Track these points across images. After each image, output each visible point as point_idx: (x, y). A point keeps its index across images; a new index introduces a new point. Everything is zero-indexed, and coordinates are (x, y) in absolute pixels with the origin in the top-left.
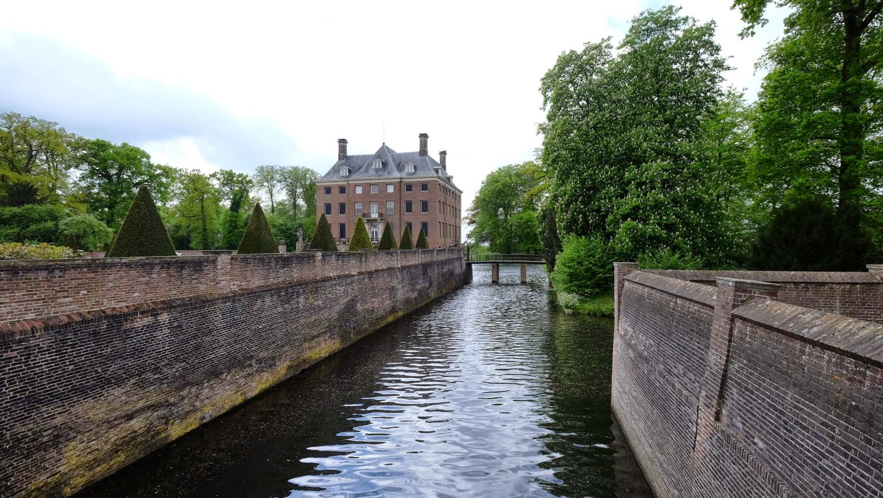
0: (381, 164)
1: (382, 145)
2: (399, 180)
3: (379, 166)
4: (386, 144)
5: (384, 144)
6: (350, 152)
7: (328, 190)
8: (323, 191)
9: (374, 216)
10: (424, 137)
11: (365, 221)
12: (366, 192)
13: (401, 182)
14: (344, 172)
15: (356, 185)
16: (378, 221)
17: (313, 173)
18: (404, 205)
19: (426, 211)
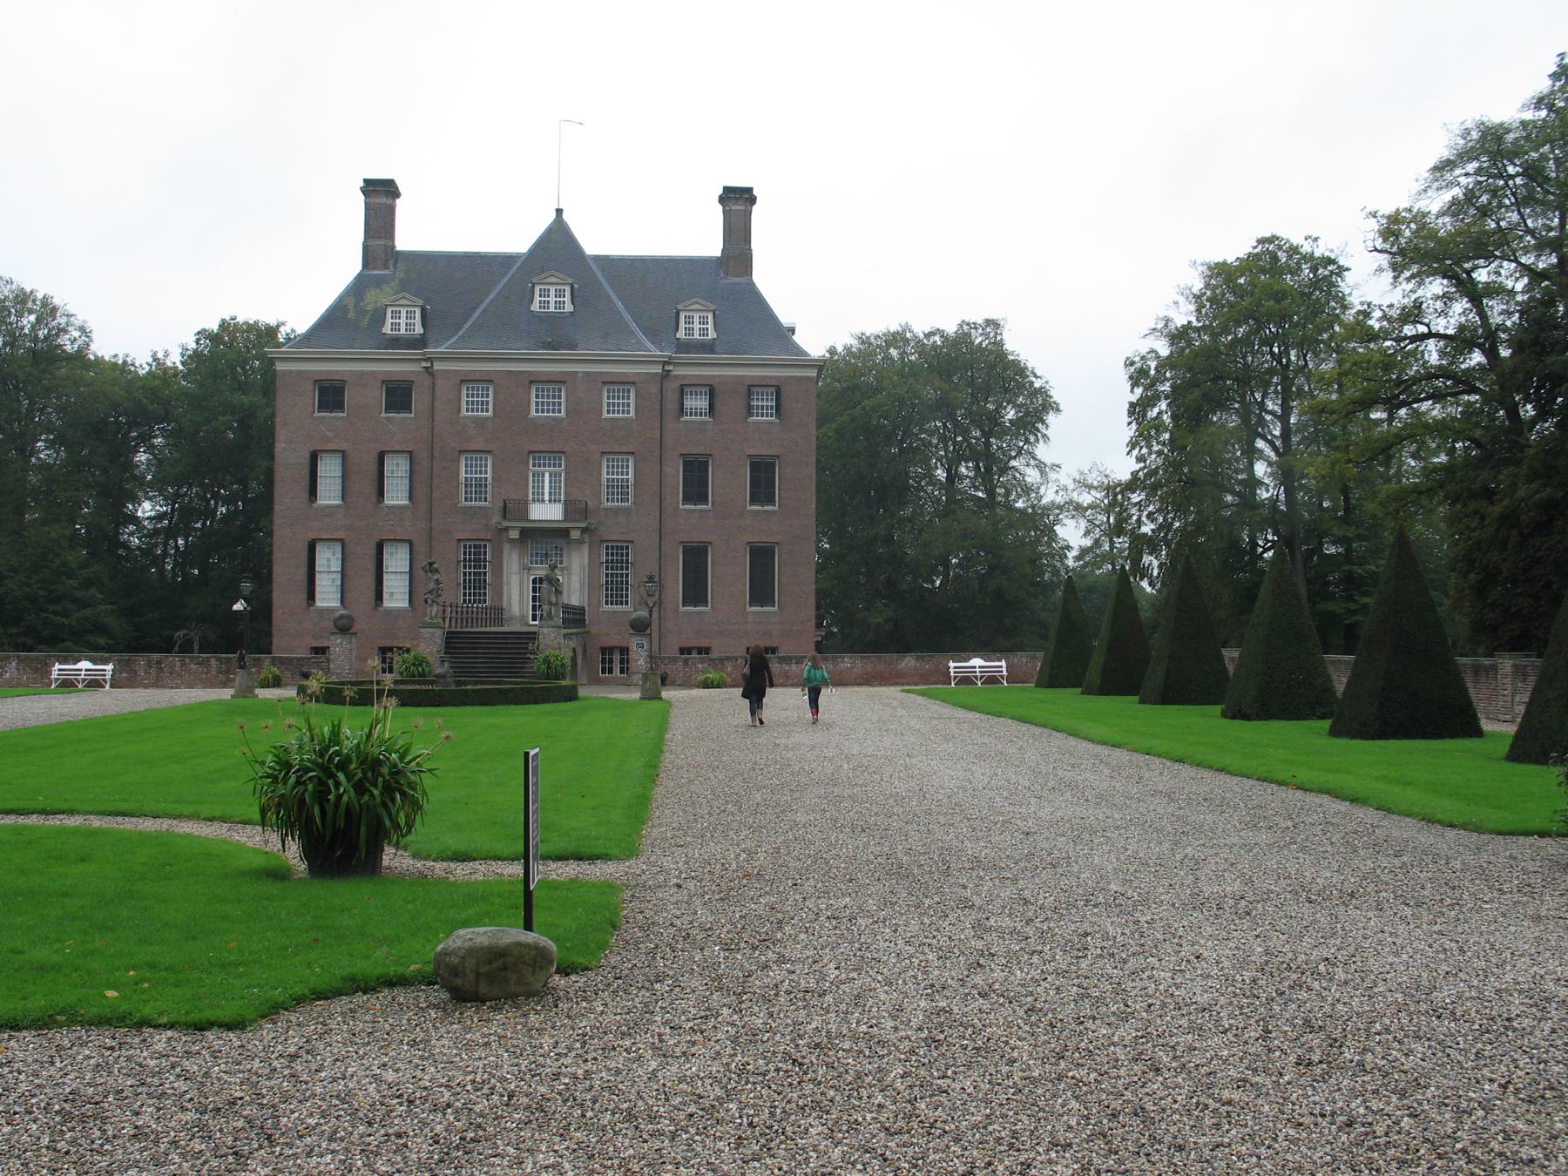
0: (567, 299)
1: (553, 215)
2: (658, 369)
3: (560, 304)
4: (565, 216)
5: (559, 212)
6: (410, 236)
7: (331, 395)
8: (312, 396)
9: (546, 512)
10: (737, 201)
11: (515, 534)
12: (512, 414)
13: (666, 375)
14: (404, 320)
15: (467, 379)
16: (575, 535)
17: (48, 310)
18: (676, 473)
19: (771, 501)
